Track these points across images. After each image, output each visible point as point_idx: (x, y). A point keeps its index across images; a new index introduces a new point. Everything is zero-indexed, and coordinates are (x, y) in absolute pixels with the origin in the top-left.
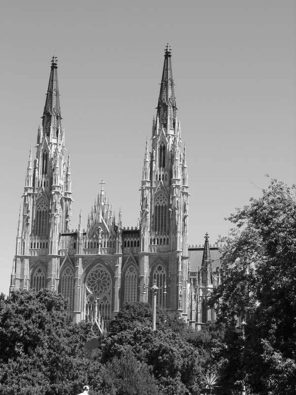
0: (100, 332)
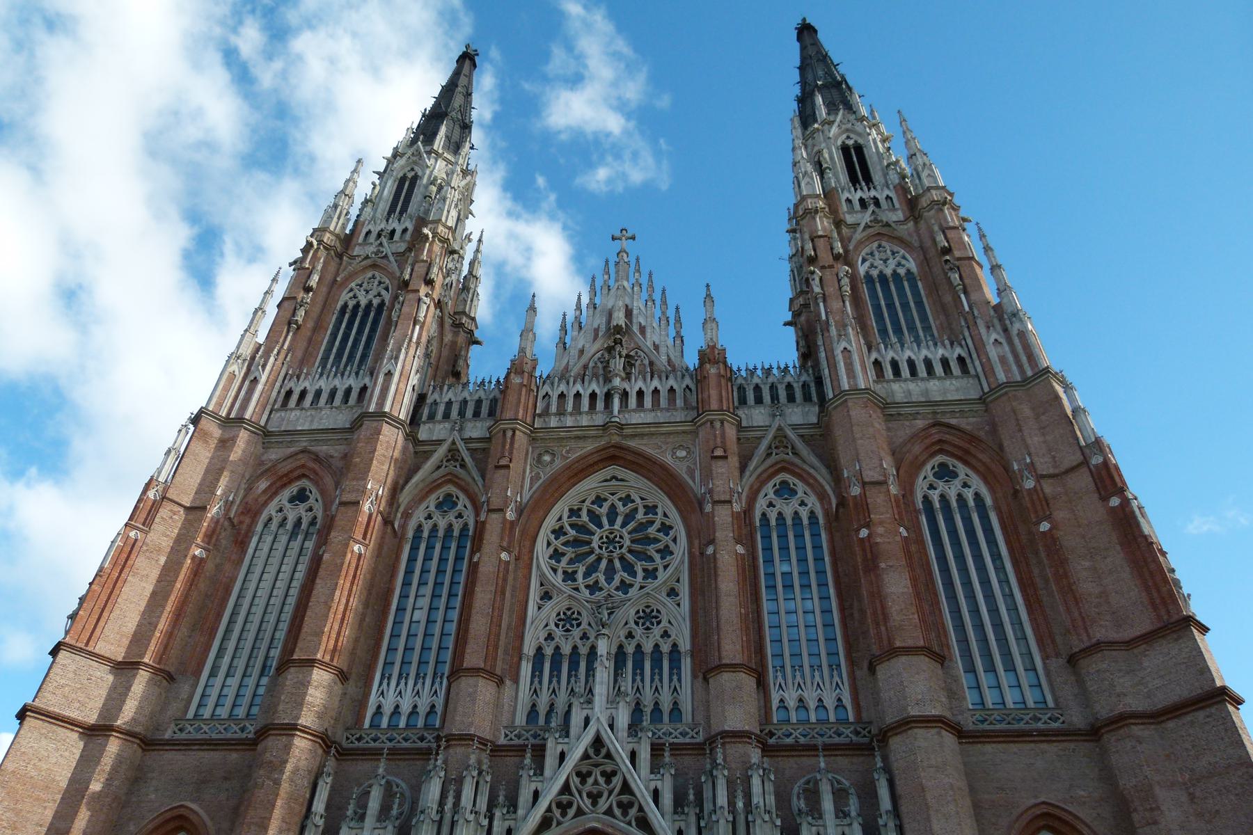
0: (626, 788)
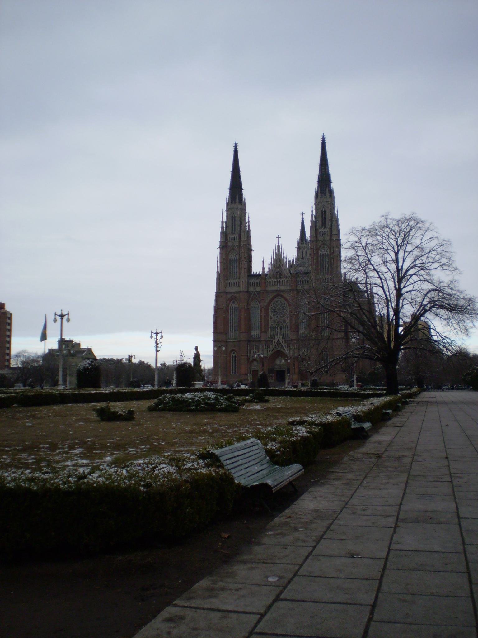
0: (282, 345)
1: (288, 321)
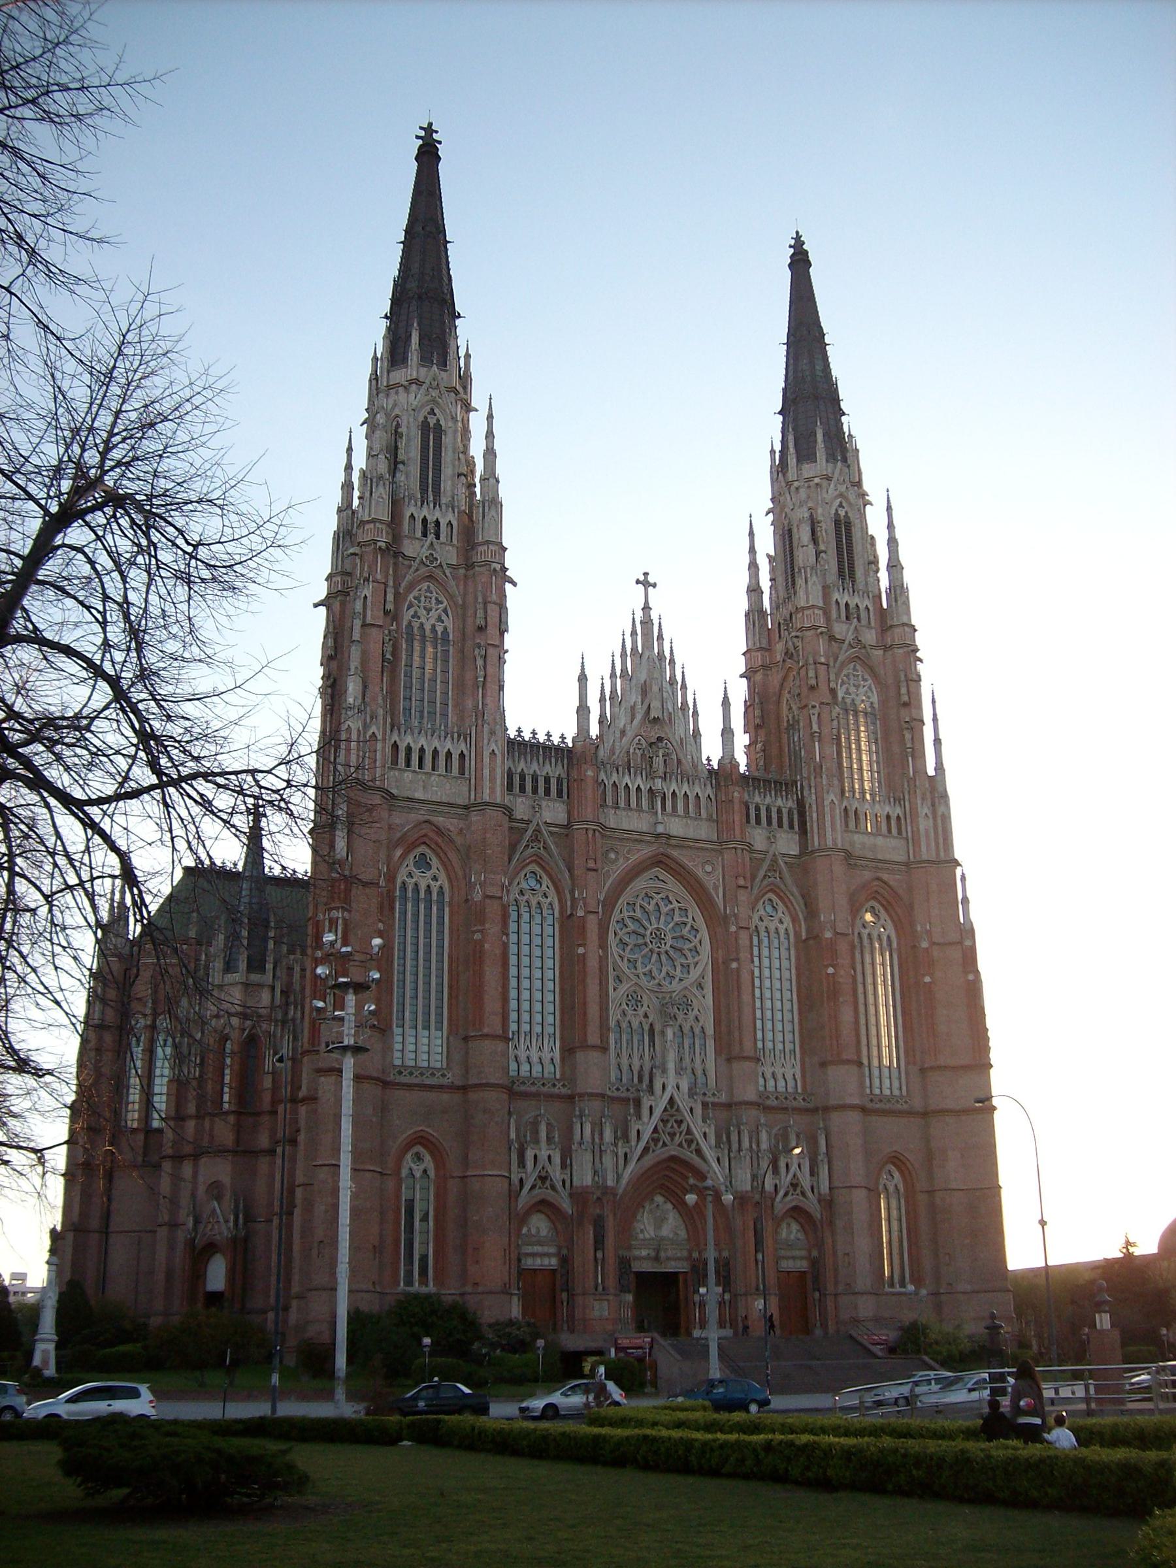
0: (689, 1132)
1: (706, 1001)
